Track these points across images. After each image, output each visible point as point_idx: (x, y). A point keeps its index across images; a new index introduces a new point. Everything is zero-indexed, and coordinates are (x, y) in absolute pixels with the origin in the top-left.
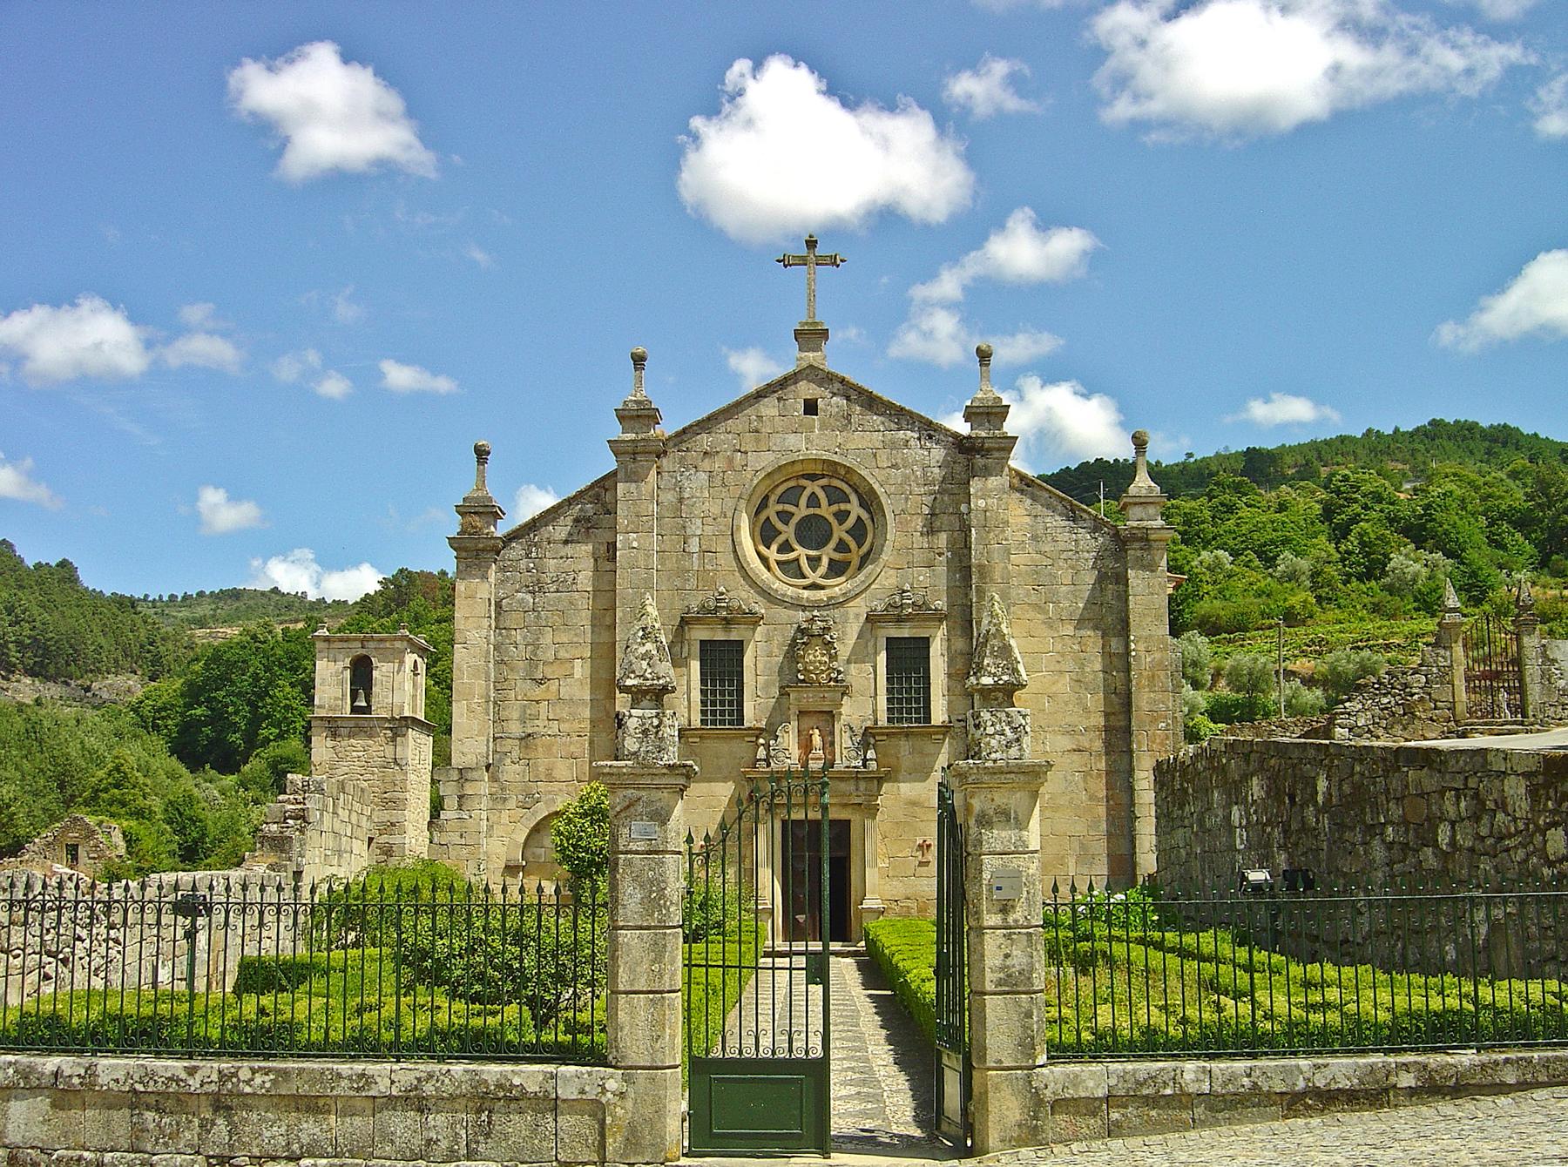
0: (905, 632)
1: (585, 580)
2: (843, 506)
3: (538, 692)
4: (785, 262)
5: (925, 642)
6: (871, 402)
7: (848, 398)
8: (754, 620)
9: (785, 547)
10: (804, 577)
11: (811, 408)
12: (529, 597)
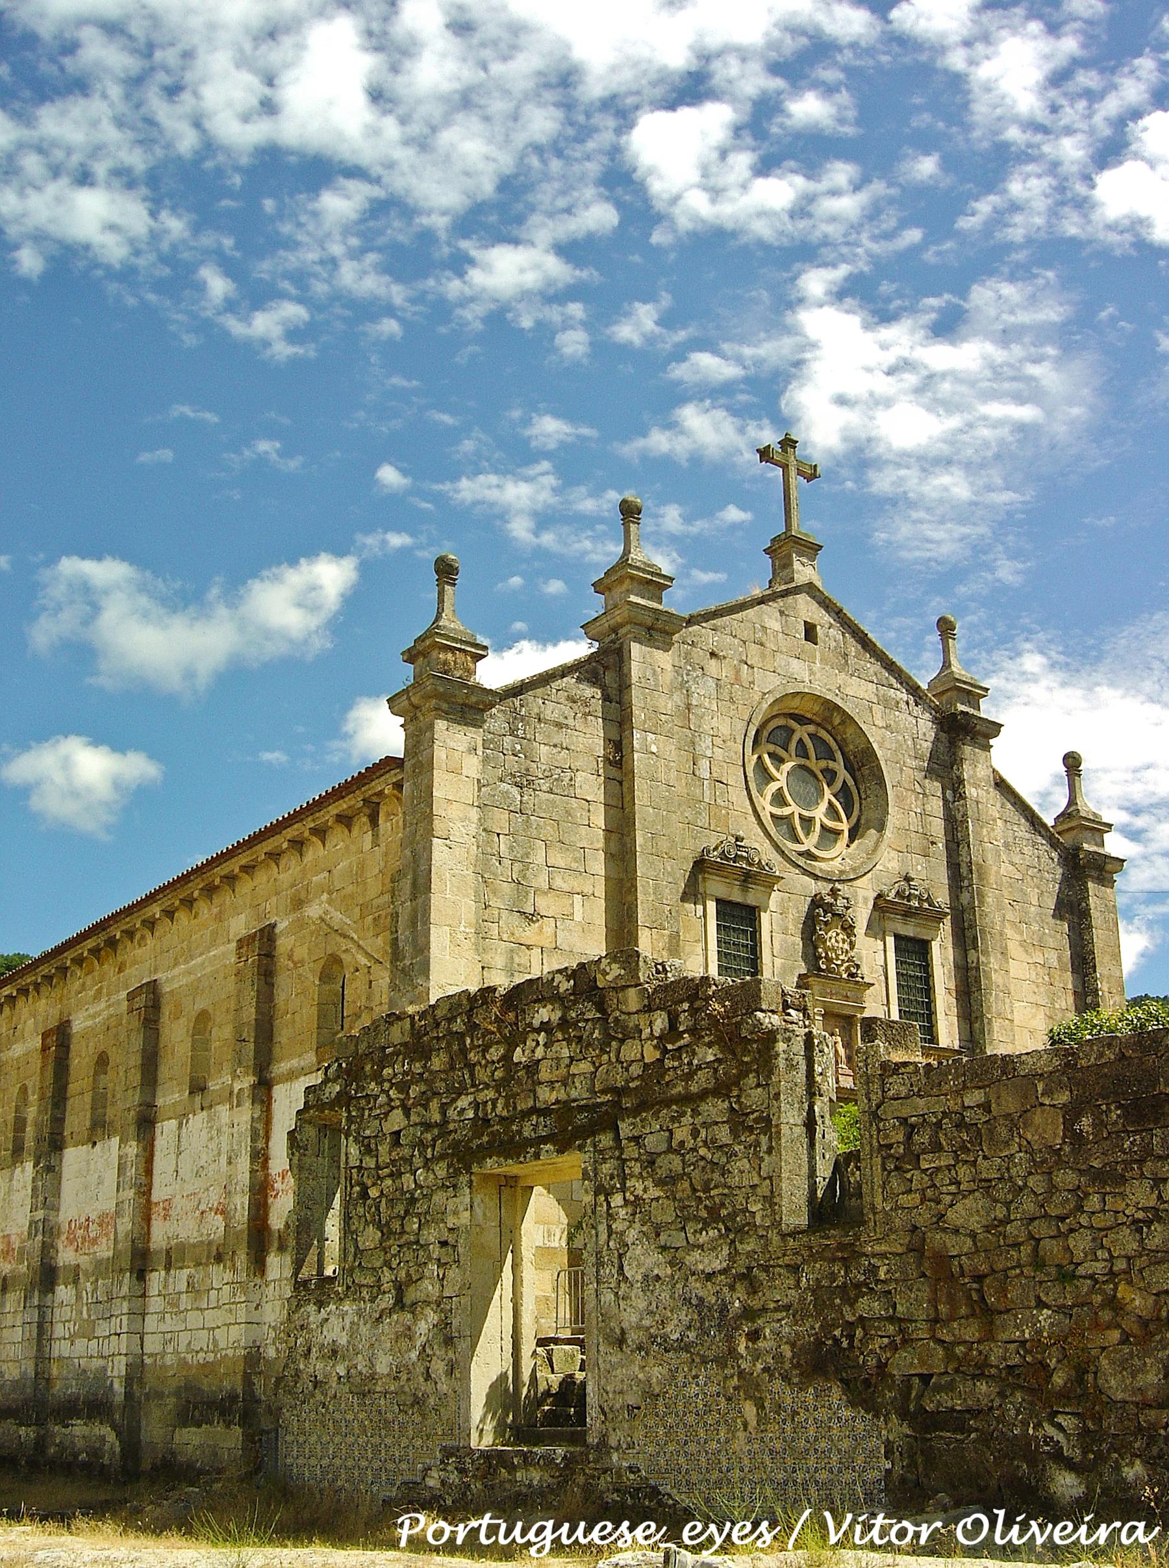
0: (909, 930)
1: (591, 787)
2: (831, 764)
3: (529, 934)
8: (769, 881)
9: (779, 799)
10: (797, 841)
11: (810, 633)
12: (515, 791)
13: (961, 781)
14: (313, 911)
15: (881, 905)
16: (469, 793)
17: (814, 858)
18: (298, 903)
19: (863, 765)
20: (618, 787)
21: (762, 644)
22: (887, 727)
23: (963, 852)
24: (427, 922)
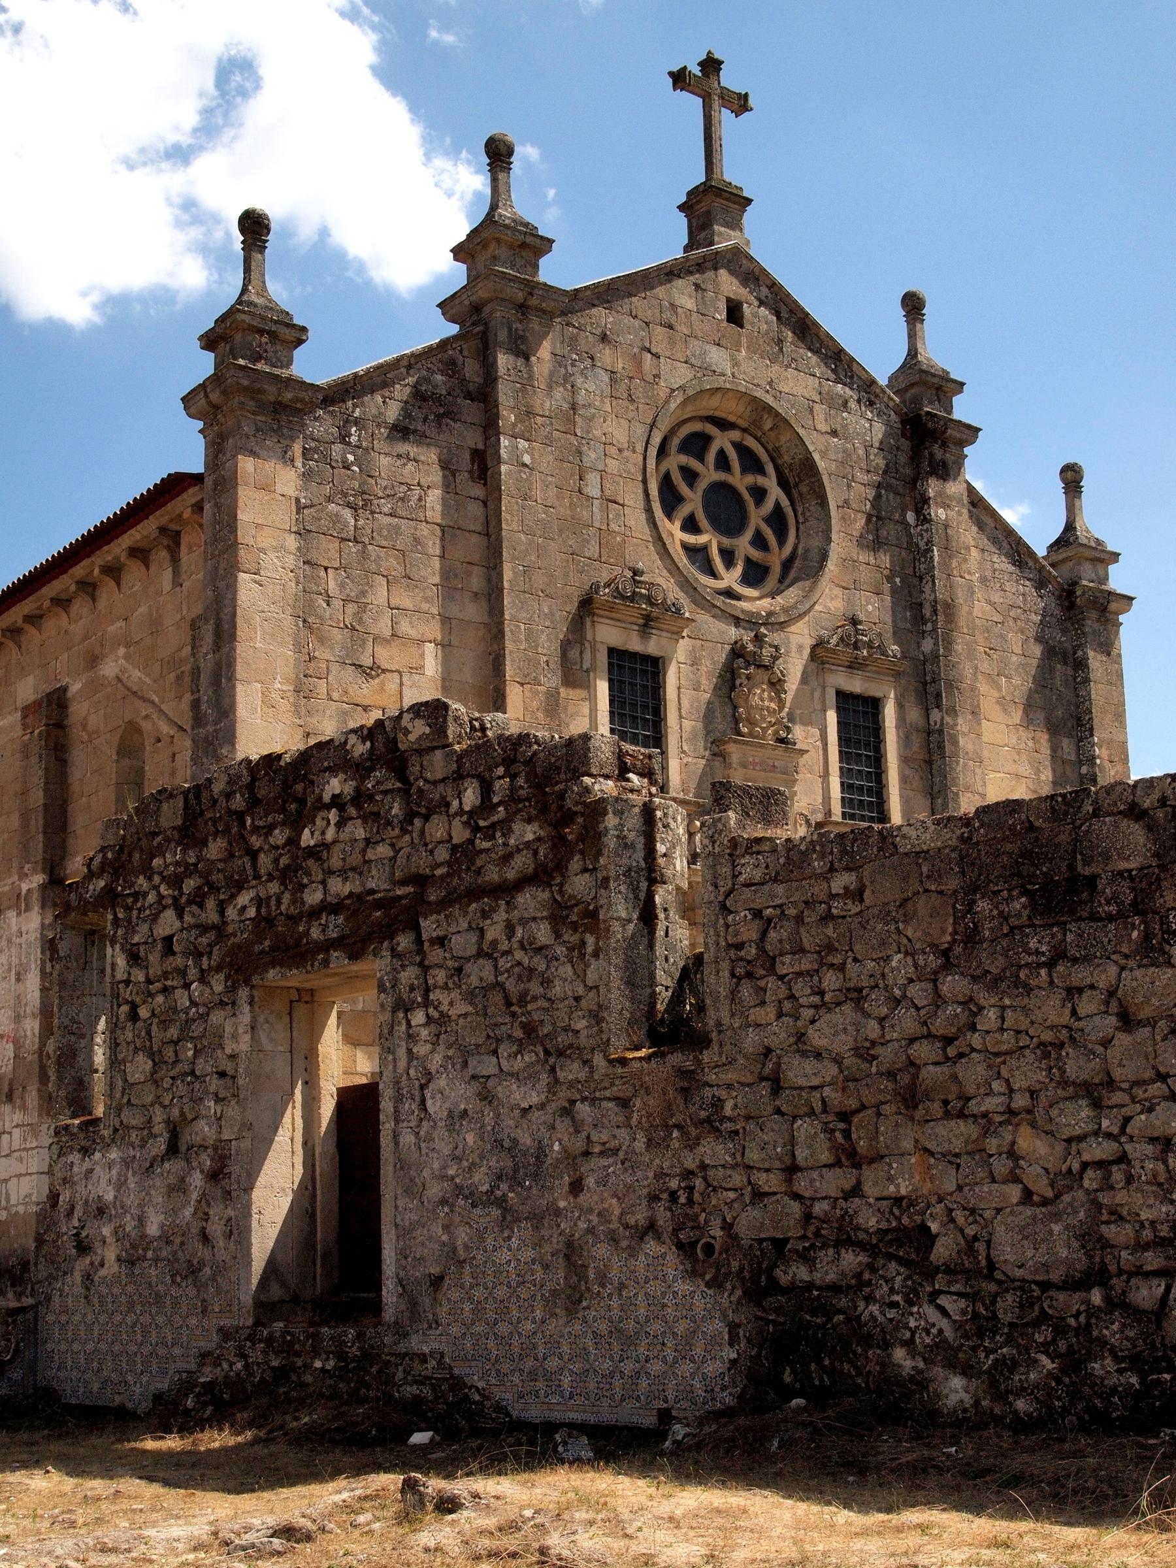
0: (856, 685)
2: (761, 481)
4: (680, 79)
5: (874, 705)
6: (804, 328)
7: (778, 314)
10: (713, 574)
11: (734, 314)
12: (347, 514)
13: (925, 501)
14: (109, 669)
15: (819, 654)
16: (285, 516)
17: (738, 597)
18: (93, 660)
19: (801, 481)
20: (482, 509)
21: (671, 327)
22: (834, 433)
23: (927, 589)
24: (231, 679)
